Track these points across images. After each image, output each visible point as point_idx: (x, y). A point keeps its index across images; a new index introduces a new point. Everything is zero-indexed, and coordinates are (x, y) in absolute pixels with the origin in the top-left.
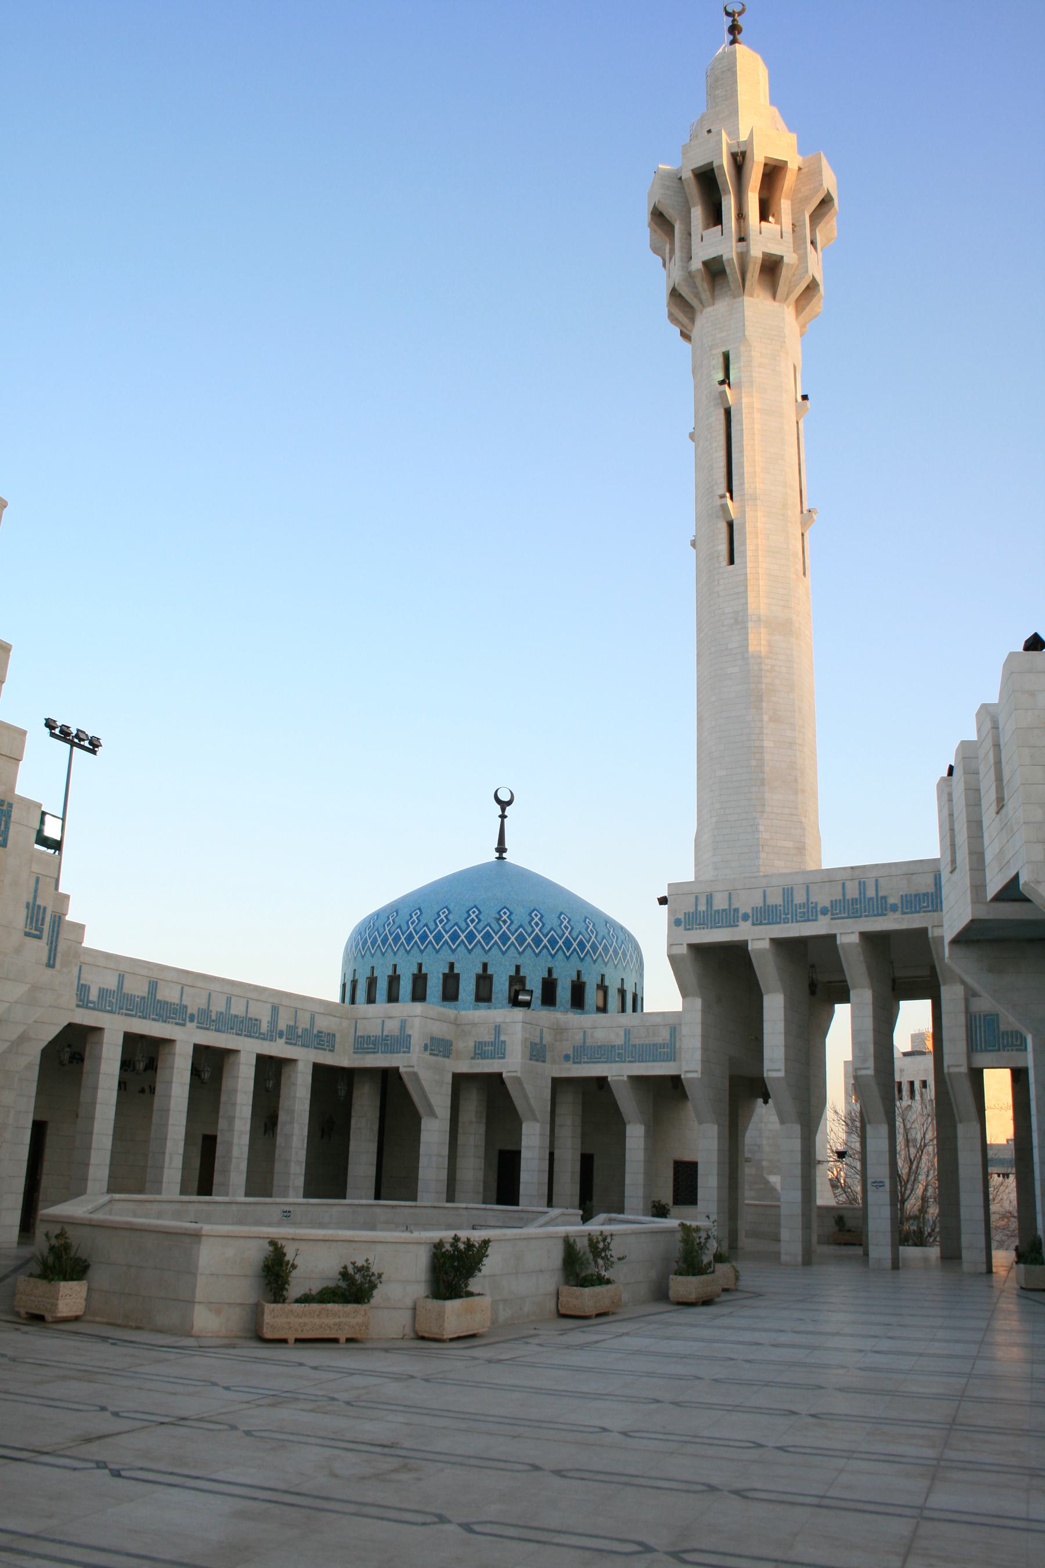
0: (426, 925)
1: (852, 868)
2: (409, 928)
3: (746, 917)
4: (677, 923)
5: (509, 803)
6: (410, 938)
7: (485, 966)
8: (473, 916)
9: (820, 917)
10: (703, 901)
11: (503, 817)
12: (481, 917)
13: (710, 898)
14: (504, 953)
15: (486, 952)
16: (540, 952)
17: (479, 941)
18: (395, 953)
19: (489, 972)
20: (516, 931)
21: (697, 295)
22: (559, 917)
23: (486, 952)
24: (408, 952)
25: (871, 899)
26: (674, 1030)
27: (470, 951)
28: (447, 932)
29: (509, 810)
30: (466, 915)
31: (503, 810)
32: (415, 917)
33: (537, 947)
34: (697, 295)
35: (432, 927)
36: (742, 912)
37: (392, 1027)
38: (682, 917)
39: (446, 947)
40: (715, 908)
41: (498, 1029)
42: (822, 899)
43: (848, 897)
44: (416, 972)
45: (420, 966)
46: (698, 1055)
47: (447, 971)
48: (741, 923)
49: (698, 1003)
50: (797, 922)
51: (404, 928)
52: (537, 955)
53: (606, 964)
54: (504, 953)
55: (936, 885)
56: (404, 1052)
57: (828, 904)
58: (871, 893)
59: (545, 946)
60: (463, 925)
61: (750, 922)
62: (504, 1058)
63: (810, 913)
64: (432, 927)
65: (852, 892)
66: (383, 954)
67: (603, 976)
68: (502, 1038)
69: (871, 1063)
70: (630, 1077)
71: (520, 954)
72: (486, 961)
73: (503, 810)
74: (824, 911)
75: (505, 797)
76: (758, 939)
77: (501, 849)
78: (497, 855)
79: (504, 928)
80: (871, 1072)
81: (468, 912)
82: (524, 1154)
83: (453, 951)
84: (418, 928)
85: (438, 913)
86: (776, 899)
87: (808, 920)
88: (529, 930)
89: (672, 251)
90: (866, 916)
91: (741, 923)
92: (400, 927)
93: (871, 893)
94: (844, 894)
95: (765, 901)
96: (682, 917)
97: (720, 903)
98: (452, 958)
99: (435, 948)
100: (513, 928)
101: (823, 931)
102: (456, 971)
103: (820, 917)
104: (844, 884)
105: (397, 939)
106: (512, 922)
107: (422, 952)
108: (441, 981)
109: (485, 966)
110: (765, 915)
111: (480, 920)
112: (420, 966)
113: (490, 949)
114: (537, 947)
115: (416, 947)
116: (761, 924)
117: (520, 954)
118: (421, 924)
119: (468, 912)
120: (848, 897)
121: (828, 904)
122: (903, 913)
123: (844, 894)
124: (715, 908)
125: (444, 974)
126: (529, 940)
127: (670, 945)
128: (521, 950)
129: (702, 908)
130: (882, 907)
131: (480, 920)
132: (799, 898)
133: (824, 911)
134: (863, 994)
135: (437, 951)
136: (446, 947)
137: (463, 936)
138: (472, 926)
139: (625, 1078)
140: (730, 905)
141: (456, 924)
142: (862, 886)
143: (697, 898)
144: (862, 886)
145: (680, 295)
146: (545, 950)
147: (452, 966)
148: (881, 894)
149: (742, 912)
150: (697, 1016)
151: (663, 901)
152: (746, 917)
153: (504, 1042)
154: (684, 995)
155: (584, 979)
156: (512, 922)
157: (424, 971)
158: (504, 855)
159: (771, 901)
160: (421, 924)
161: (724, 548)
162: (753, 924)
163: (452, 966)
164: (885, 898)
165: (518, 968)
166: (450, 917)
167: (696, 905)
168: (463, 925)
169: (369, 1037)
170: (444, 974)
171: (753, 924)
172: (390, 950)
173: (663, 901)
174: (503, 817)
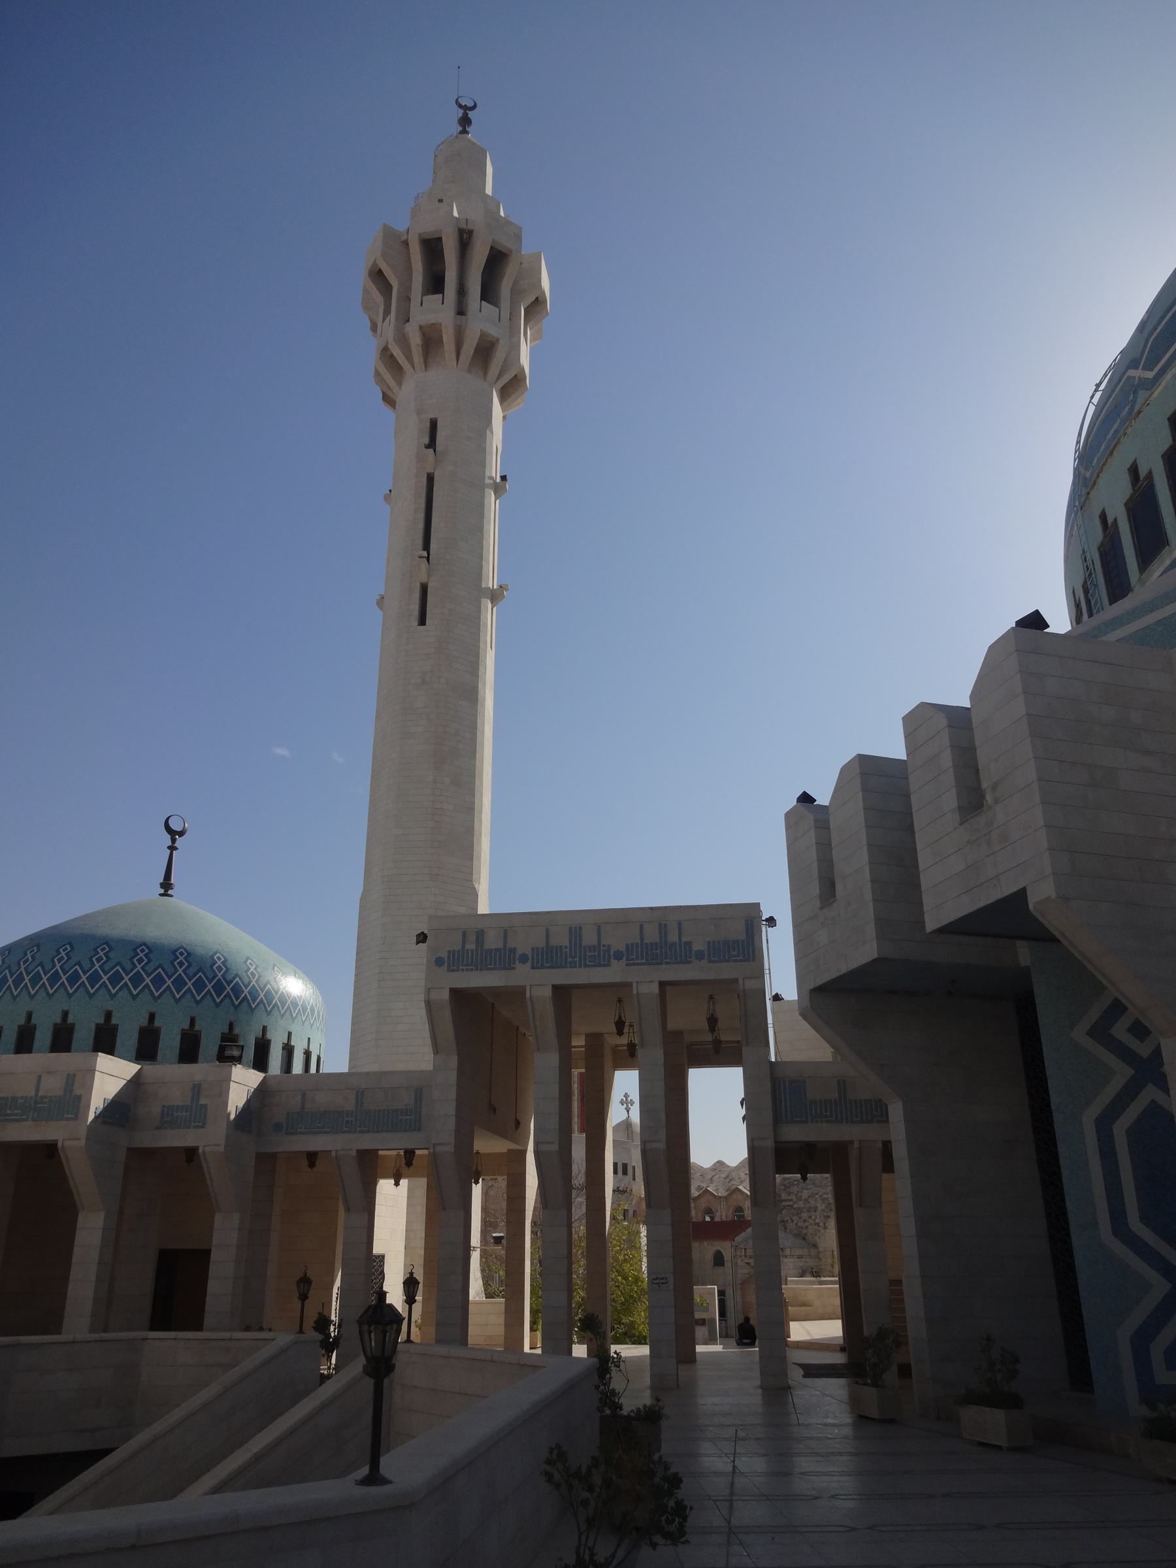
0: (79, 963)
1: (651, 908)
2: (54, 966)
3: (524, 959)
4: (439, 962)
5: (181, 834)
6: (55, 978)
7: (152, 1017)
8: (141, 955)
9: (614, 962)
10: (472, 938)
11: (172, 848)
12: (151, 956)
13: (480, 935)
14: (177, 1001)
15: (156, 999)
16: (221, 1001)
17: (147, 986)
18: (32, 997)
19: (157, 1023)
20: (195, 974)
21: (409, 358)
22: (245, 962)
23: (156, 999)
24: (50, 996)
25: (673, 944)
26: (419, 1093)
27: (134, 997)
28: (106, 974)
29: (180, 841)
30: (132, 954)
31: (174, 841)
32: (63, 954)
33: (218, 996)
34: (409, 358)
35: (86, 965)
36: (519, 952)
37: (53, 1086)
38: (444, 955)
39: (103, 990)
40: (486, 947)
41: (197, 1090)
42: (616, 941)
43: (647, 941)
44: (59, 1021)
45: (65, 1014)
46: (451, 1124)
47: (102, 1021)
48: (518, 965)
49: (454, 1061)
50: (586, 966)
51: (48, 966)
52: (217, 1005)
53: (293, 1019)
54: (177, 1001)
55: (747, 933)
56: (68, 1119)
57: (623, 948)
58: (673, 937)
59: (228, 995)
60: (128, 966)
61: (529, 964)
62: (203, 1127)
63: (601, 956)
64: (86, 965)
65: (652, 935)
66: (14, 998)
67: (290, 1034)
68: (202, 1101)
69: (662, 1134)
70: (358, 1151)
71: (198, 1002)
72: (153, 1010)
73: (174, 841)
74: (618, 956)
75: (176, 825)
76: (539, 985)
77: (167, 885)
78: (162, 891)
79: (180, 971)
80: (661, 1146)
81: (135, 950)
82: (215, 1256)
83: (113, 996)
84: (66, 967)
85: (95, 950)
86: (561, 939)
87: (600, 965)
88: (210, 976)
89: (387, 312)
90: (667, 963)
91: (518, 965)
92: (41, 964)
93: (673, 937)
94: (642, 939)
95: (547, 941)
96: (444, 955)
97: (492, 941)
98: (110, 1005)
99: (88, 992)
100: (191, 971)
101: (617, 979)
102: (114, 1021)
103: (614, 962)
104: (641, 926)
105: (36, 979)
106: (190, 965)
107: (70, 996)
108: (93, 1033)
109: (152, 1017)
110: (547, 957)
111: (150, 960)
112: (65, 1014)
113: (161, 995)
114: (218, 996)
115: (62, 990)
116: (542, 967)
117: (198, 1002)
118: (72, 962)
119: (135, 950)
120: (647, 941)
121: (623, 948)
122: (710, 962)
123: (642, 939)
124: (486, 947)
125: (97, 1025)
126: (209, 987)
127: (428, 990)
128: (198, 998)
129: (471, 946)
130: (683, 953)
131: (150, 960)
132: (589, 939)
133: (618, 956)
134: (655, 1054)
135: (91, 996)
136: (103, 990)
137: (126, 979)
138: (139, 967)
139: (354, 1154)
140: (505, 944)
141: (119, 964)
142: (663, 928)
143: (464, 934)
144: (663, 928)
145: (392, 356)
146: (227, 1001)
147: (109, 1015)
148: (684, 940)
149: (519, 952)
150: (453, 1076)
151: (422, 938)
152: (524, 959)
153: (205, 1106)
154: (436, 1050)
155: (269, 1036)
156: (190, 965)
157: (70, 1020)
158: (170, 892)
159: (555, 941)
160: (72, 962)
161: (416, 608)
162: (533, 967)
163: (109, 1015)
164: (689, 944)
165: (193, 1021)
166: (111, 955)
167: (464, 943)
168: (128, 966)
169: (14, 1099)
170: (97, 1025)
171: (533, 967)
172: (25, 993)
173: (422, 938)
174: (172, 848)
